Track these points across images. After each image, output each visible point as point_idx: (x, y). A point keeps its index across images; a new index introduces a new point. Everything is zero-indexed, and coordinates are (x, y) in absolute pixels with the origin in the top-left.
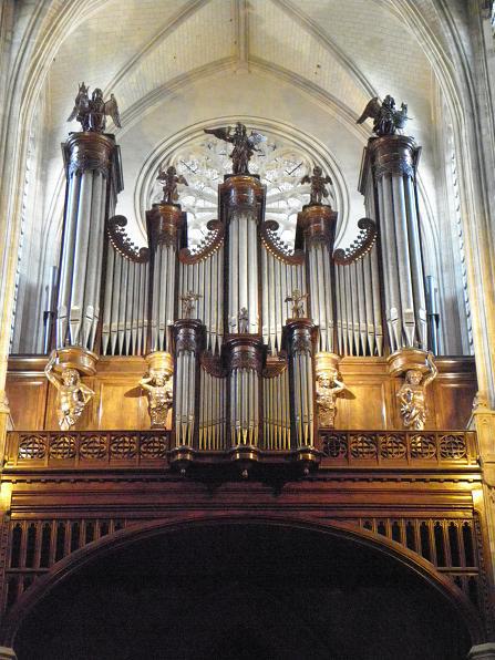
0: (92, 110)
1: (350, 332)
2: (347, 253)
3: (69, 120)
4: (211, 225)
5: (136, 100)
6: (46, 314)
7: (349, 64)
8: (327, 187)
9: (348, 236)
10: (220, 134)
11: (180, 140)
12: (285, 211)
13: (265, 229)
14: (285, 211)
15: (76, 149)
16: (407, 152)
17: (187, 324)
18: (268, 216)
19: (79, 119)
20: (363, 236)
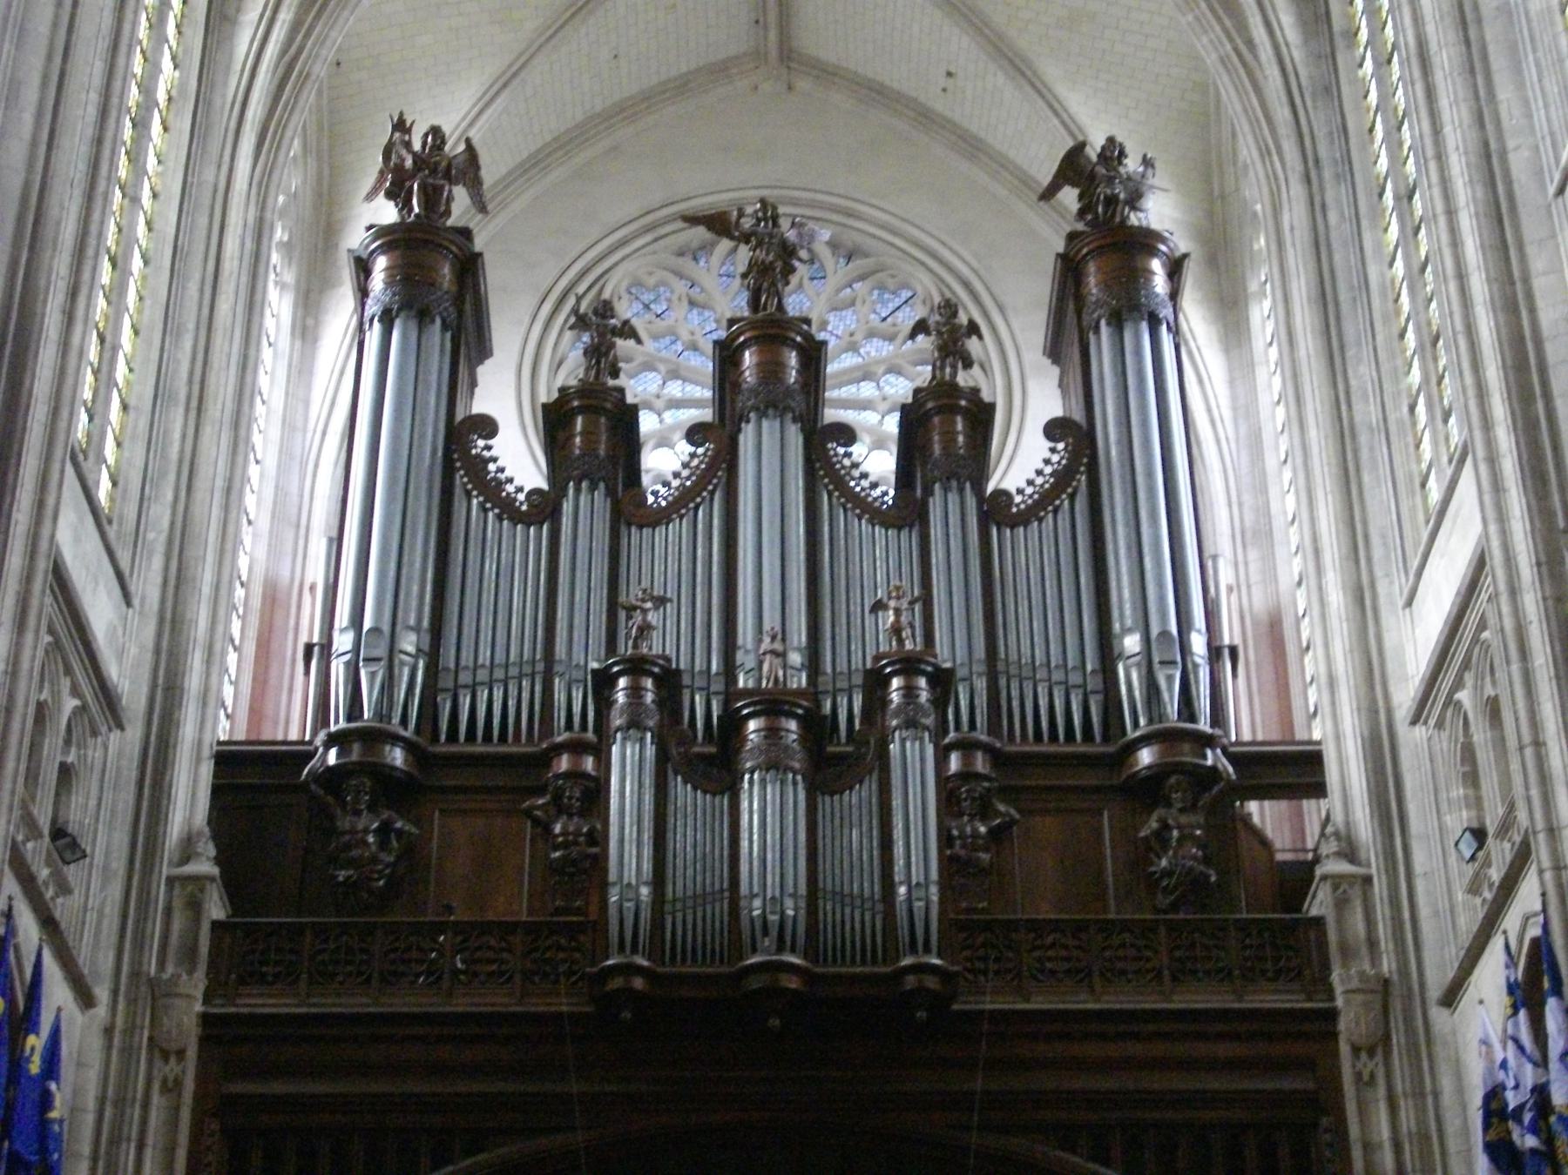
2: (1018, 499)
3: (370, 197)
4: (695, 434)
5: (525, 155)
6: (309, 648)
7: (1020, 68)
8: (973, 345)
9: (1022, 461)
10: (719, 224)
11: (623, 243)
12: (871, 409)
13: (824, 442)
14: (871, 409)
15: (381, 262)
16: (1156, 265)
17: (636, 666)
18: (831, 415)
19: (390, 195)
20: (1055, 458)
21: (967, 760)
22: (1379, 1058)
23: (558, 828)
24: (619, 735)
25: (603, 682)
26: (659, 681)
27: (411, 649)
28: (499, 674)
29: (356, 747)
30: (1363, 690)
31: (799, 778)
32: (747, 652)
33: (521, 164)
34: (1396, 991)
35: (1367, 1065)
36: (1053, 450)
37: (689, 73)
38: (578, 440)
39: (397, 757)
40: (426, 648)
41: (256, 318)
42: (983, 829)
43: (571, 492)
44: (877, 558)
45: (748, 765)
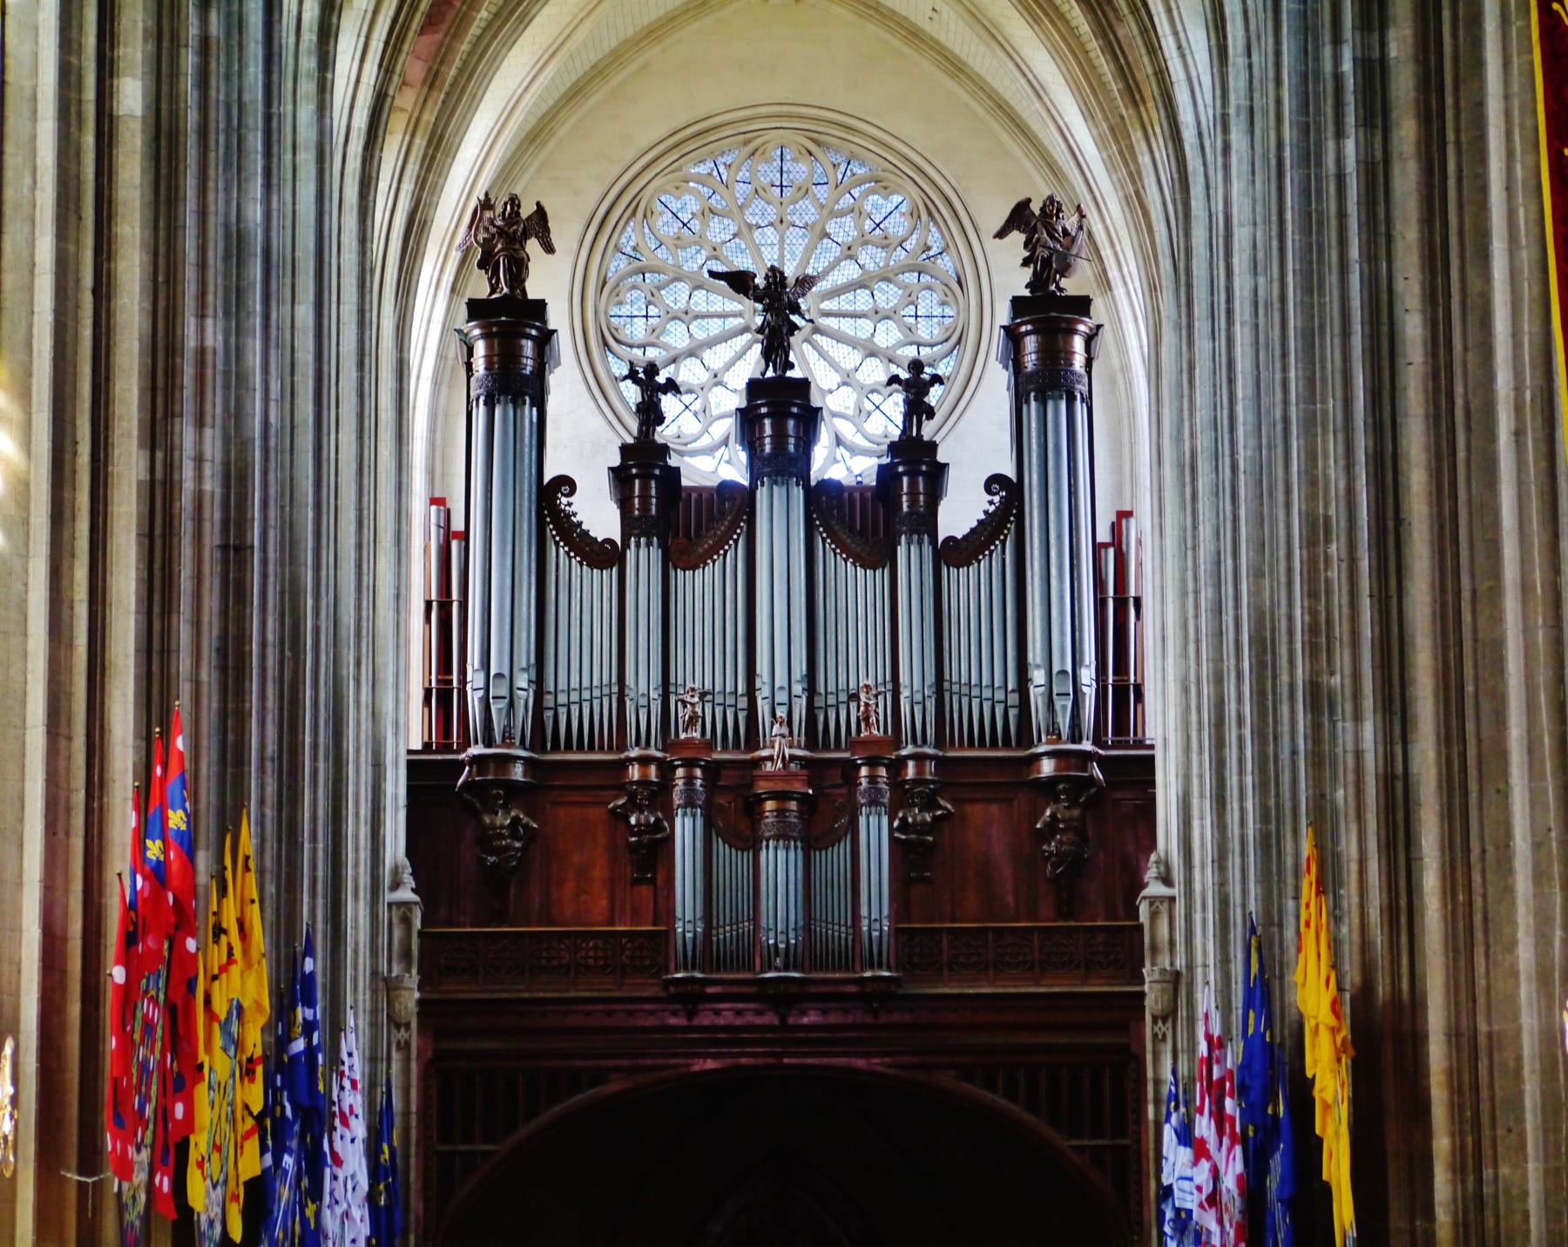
0: (507, 236)
1: (965, 700)
10: (739, 282)
15: (480, 348)
16: (1078, 343)
19: (481, 265)
21: (920, 769)
22: (1169, 1024)
25: (666, 769)
27: (524, 685)
28: (586, 695)
29: (492, 766)
30: (1181, 759)
33: (566, 94)
34: (1183, 981)
35: (1164, 1028)
36: (991, 503)
39: (518, 773)
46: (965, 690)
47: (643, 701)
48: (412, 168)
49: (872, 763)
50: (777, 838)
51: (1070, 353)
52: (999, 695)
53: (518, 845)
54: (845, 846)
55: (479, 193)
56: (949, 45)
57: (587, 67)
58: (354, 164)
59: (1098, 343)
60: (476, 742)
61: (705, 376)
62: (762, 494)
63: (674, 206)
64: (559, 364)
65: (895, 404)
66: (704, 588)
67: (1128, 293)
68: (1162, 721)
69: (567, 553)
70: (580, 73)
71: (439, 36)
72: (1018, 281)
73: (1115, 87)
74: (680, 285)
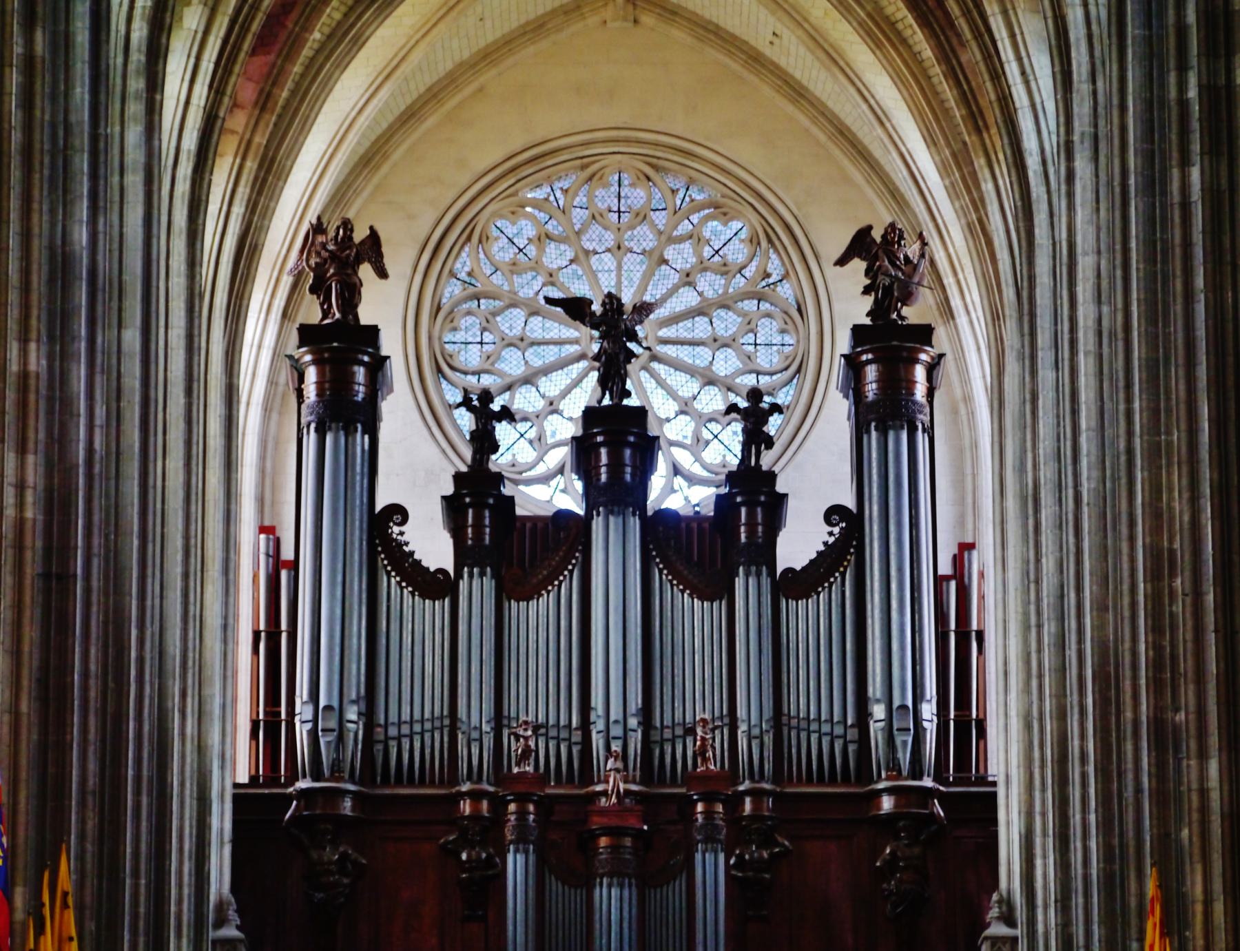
0: (339, 259)
1: (803, 735)
5: (403, 108)
10: (576, 308)
15: (311, 374)
16: (920, 373)
21: (756, 805)
23: (464, 856)
24: (512, 847)
25: (498, 804)
26: (536, 803)
27: (354, 717)
28: (417, 728)
30: (1023, 797)
31: (633, 881)
32: (598, 717)
33: (399, 118)
36: (831, 534)
37: (543, 15)
38: (470, 530)
40: (363, 710)
41: (233, 475)
42: (765, 855)
43: (466, 576)
44: (692, 617)
45: (601, 871)
46: (803, 724)
47: (475, 735)
48: (243, 191)
49: (709, 799)
50: (611, 875)
51: (912, 383)
52: (839, 730)
53: (346, 881)
54: (680, 884)
55: (311, 217)
56: (790, 70)
57: (422, 89)
58: (183, 187)
59: (940, 373)
60: (304, 776)
61: (540, 404)
62: (597, 524)
63: (510, 230)
64: (391, 390)
65: (733, 435)
66: (536, 617)
67: (971, 322)
68: (1004, 756)
69: (399, 583)
70: (415, 96)
71: (272, 57)
72: (859, 310)
73: (958, 114)
74: (516, 311)
